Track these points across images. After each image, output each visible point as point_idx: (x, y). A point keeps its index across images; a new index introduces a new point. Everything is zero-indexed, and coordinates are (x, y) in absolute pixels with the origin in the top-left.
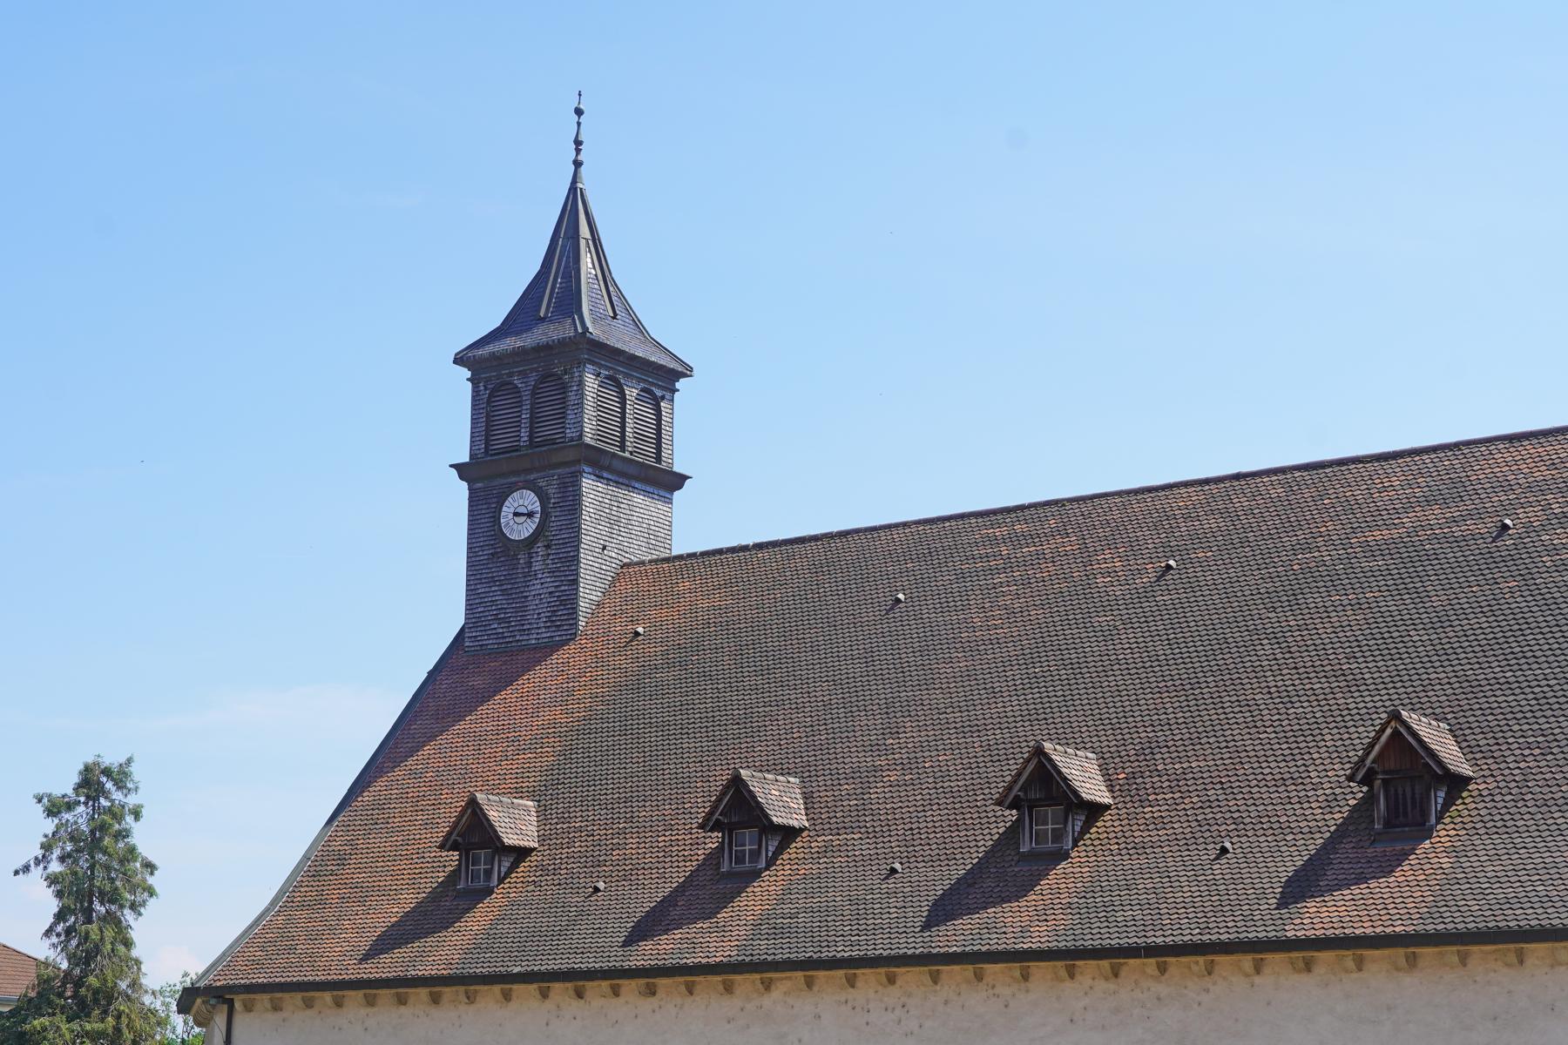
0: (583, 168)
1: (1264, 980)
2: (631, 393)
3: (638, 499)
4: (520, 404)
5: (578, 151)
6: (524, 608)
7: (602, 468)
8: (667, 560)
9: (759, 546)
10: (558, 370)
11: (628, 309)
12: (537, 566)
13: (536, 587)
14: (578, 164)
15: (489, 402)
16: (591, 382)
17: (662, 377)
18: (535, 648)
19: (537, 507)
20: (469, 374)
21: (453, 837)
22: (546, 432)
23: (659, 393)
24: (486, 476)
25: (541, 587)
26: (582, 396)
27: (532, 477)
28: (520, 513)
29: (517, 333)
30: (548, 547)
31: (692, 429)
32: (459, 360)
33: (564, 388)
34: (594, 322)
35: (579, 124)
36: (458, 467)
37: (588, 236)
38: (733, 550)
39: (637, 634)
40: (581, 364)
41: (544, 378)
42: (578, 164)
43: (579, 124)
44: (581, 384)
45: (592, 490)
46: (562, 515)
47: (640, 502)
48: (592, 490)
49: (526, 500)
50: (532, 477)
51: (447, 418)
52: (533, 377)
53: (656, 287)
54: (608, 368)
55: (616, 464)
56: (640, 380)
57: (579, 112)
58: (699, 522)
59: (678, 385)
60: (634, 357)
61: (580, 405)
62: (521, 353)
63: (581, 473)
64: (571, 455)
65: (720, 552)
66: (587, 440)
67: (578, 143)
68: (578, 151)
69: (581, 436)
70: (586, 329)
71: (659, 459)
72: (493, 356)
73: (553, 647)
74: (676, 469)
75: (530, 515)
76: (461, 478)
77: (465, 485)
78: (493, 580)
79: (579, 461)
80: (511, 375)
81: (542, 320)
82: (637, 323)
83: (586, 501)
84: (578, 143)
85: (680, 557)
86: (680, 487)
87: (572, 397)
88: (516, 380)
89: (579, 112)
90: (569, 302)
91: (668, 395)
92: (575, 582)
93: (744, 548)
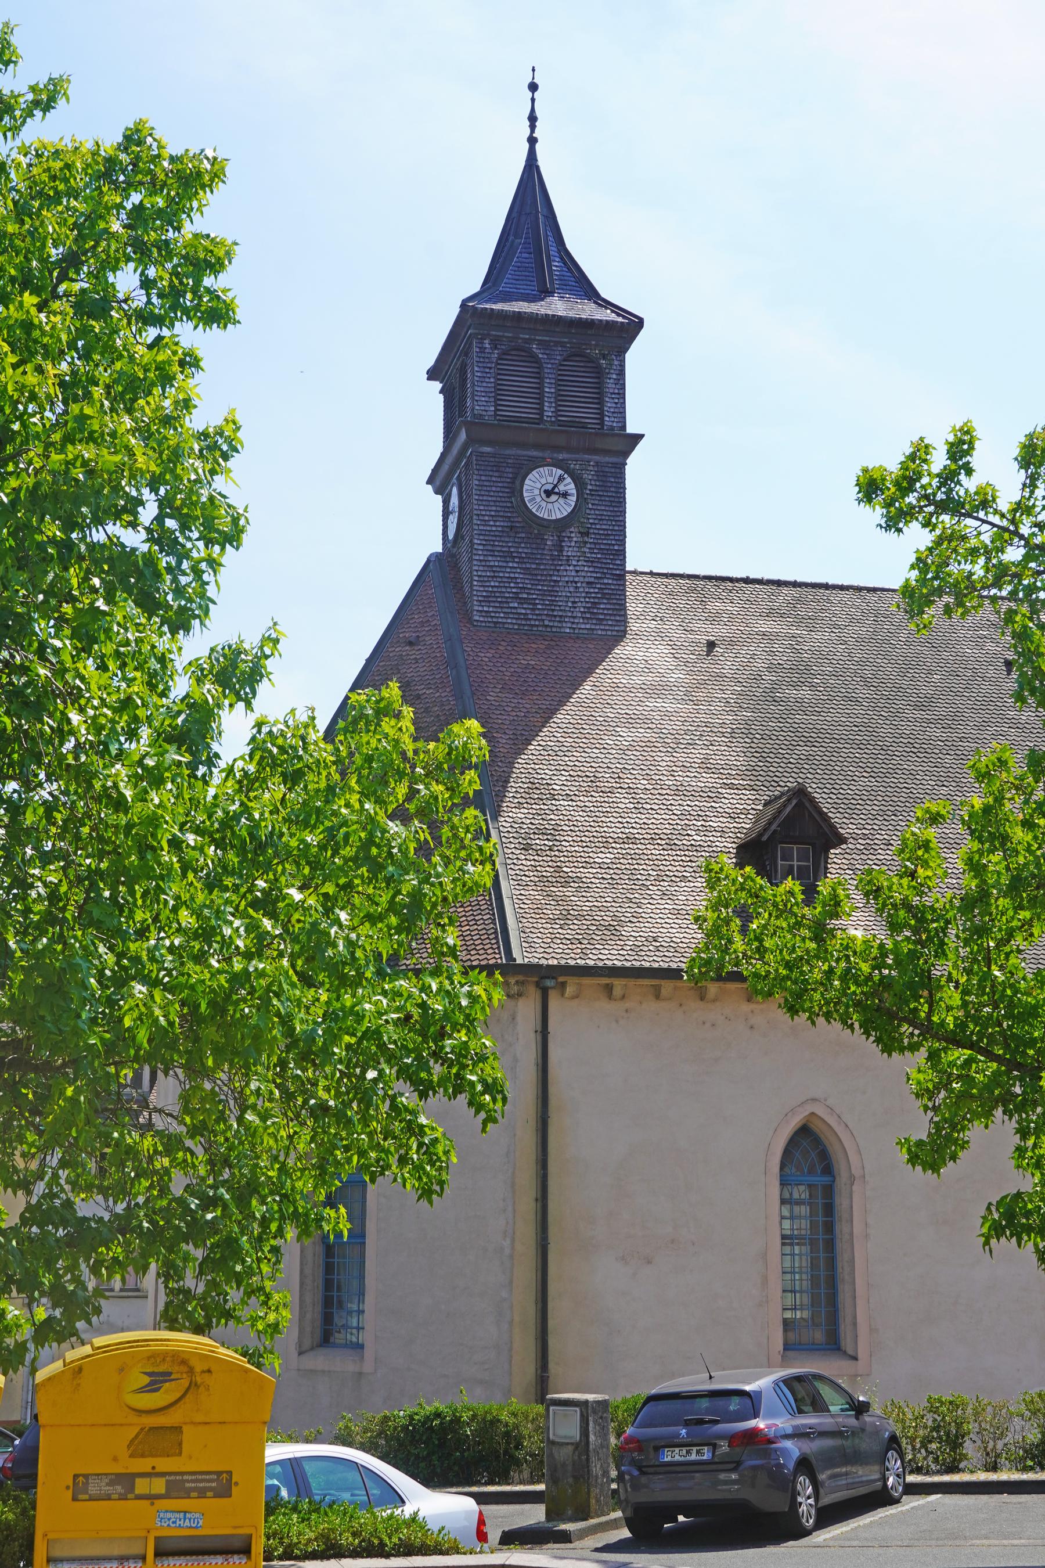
1: (532, 1035)
4: (539, 376)
5: (533, 127)
6: (552, 593)
12: (568, 552)
13: (569, 573)
14: (532, 141)
21: (774, 827)
33: (599, 374)
35: (533, 100)
42: (532, 141)
43: (533, 100)
57: (533, 87)
67: (533, 119)
68: (533, 127)
78: (509, 556)
84: (533, 119)
87: (610, 385)
89: (533, 87)
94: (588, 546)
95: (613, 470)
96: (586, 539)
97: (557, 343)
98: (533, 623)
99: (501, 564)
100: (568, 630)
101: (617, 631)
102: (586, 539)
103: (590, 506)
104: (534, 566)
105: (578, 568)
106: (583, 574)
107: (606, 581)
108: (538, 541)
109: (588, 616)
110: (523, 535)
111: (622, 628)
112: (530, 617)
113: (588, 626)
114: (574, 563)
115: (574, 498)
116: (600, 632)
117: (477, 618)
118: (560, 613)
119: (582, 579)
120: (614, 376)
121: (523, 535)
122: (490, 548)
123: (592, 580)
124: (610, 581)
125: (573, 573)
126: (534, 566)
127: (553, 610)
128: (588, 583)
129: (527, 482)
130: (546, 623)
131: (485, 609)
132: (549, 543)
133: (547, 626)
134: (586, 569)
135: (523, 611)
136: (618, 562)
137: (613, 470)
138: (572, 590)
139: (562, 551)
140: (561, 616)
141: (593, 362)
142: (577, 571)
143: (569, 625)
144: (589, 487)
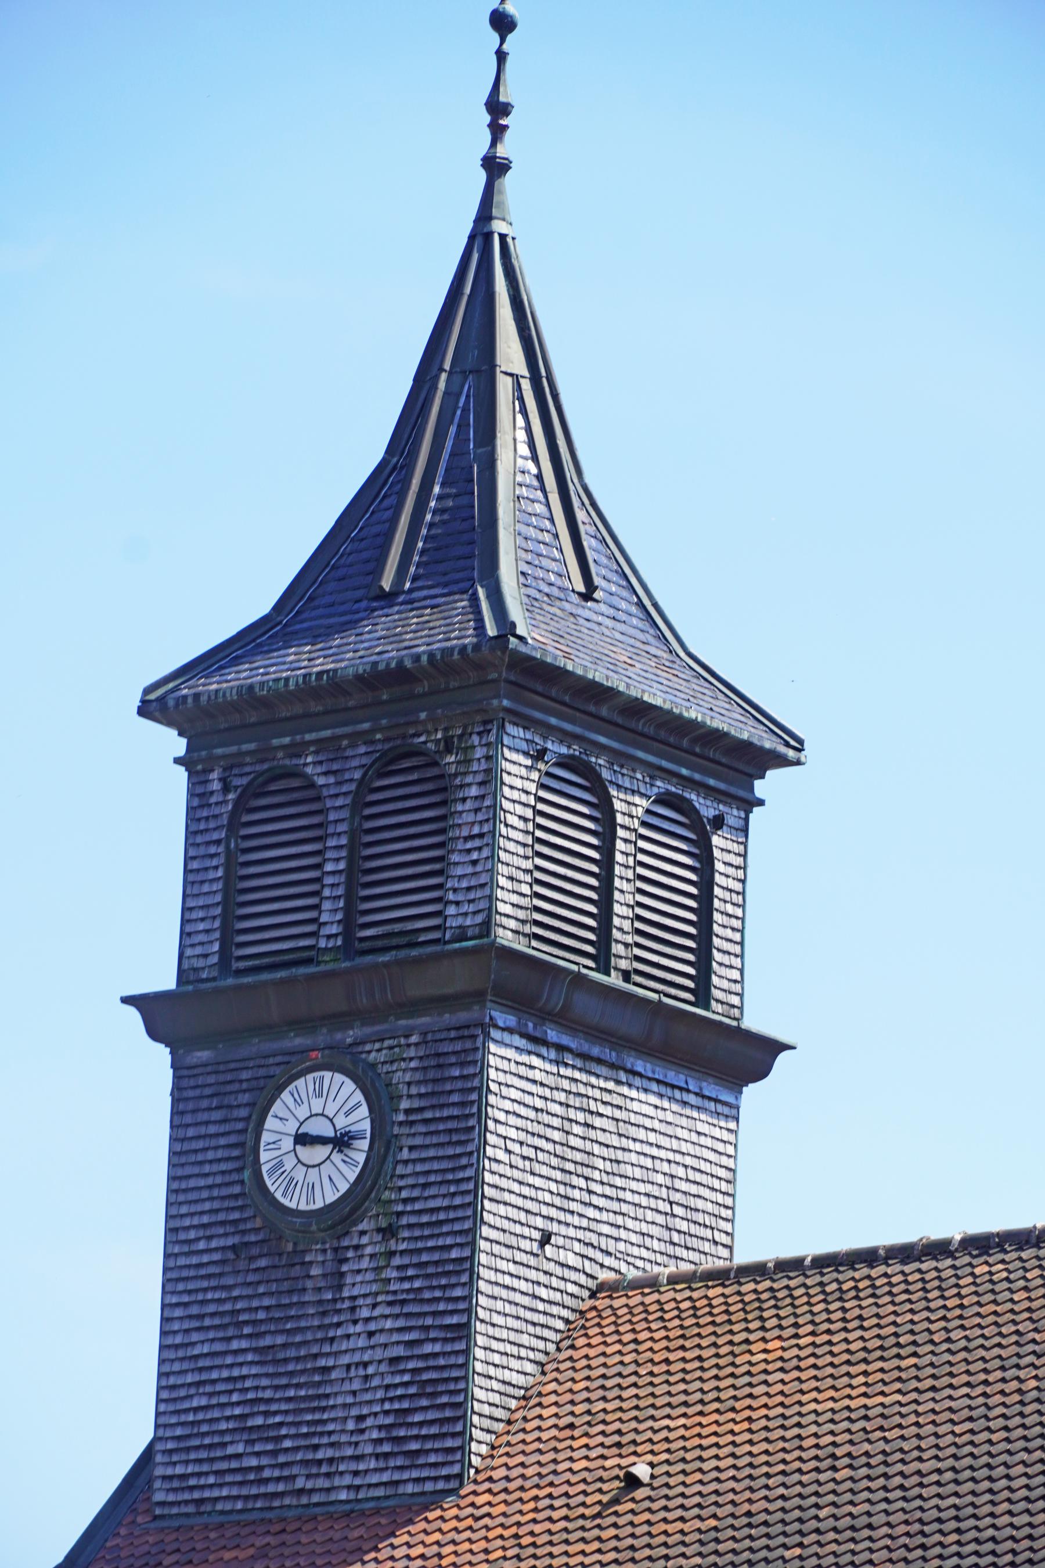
0: (509, 182)
2: (630, 807)
3: (643, 1103)
4: (320, 833)
5: (497, 131)
6: (318, 1402)
7: (546, 1016)
8: (719, 1276)
9: (980, 1245)
10: (429, 740)
11: (627, 574)
12: (356, 1286)
13: (354, 1343)
14: (495, 167)
15: (234, 824)
16: (518, 776)
17: (716, 766)
18: (350, 1514)
19: (361, 1120)
20: (179, 746)
22: (390, 910)
23: (707, 809)
24: (222, 1026)
25: (366, 1343)
26: (493, 813)
27: (350, 1036)
28: (314, 1138)
29: (316, 636)
30: (388, 1232)
31: (800, 913)
32: (154, 706)
33: (443, 791)
34: (531, 606)
35: (501, 56)
36: (143, 1003)
37: (520, 367)
38: (905, 1253)
39: (632, 1482)
40: (491, 723)
41: (386, 764)
42: (495, 167)
43: (501, 56)
44: (491, 779)
45: (514, 1074)
46: (431, 1142)
47: (648, 1115)
48: (514, 1074)
49: (332, 1100)
50: (350, 1036)
51: (120, 863)
52: (359, 757)
53: (702, 511)
54: (565, 737)
55: (584, 1005)
56: (655, 772)
57: (502, 23)
58: (807, 1174)
59: (760, 788)
60: (639, 709)
61: (488, 839)
62: (329, 689)
63: (485, 1027)
64: (459, 978)
65: (869, 1257)
66: (505, 937)
67: (497, 109)
68: (497, 131)
69: (486, 927)
70: (507, 628)
71: (702, 993)
72: (248, 697)
73: (398, 1512)
74: (752, 1022)
75: (342, 1142)
76: (154, 1033)
77: (162, 1053)
79: (478, 997)
80: (296, 750)
81: (388, 598)
82: (650, 614)
83: (498, 1106)
84: (497, 109)
85: (757, 1270)
86: (761, 1072)
87: (465, 815)
88: (310, 765)
89: (502, 23)
90: (463, 549)
91: (733, 816)
92: (463, 1332)
93: (939, 1249)
94: (397, 1261)
95: (458, 1046)
96: (393, 1245)
97: (355, 738)
98: (271, 1488)
99: (218, 1347)
100: (343, 1496)
101: (447, 1478)
102: (393, 1245)
103: (405, 1154)
104: (280, 1340)
105: (372, 1326)
106: (382, 1339)
107: (428, 1348)
108: (296, 1271)
109: (386, 1448)
110: (263, 1263)
111: (456, 1469)
112: (267, 1473)
113: (385, 1477)
114: (365, 1313)
115: (365, 1144)
116: (410, 1488)
117: (159, 1497)
118: (330, 1453)
119: (379, 1354)
120: (474, 791)
121: (263, 1263)
122: (195, 1310)
123: (400, 1351)
124: (438, 1348)
125: (361, 1342)
126: (280, 1340)
127: (316, 1447)
128: (394, 1360)
129: (270, 1123)
130: (300, 1483)
131: (179, 1470)
132: (315, 1271)
133: (301, 1491)
134: (389, 1324)
135: (254, 1462)
136: (458, 1292)
137: (458, 1046)
138: (356, 1385)
139: (340, 1287)
140: (331, 1461)
141: (435, 764)
142: (371, 1334)
143: (347, 1480)
144: (405, 1104)
